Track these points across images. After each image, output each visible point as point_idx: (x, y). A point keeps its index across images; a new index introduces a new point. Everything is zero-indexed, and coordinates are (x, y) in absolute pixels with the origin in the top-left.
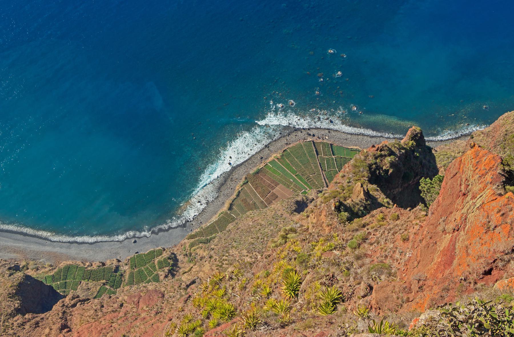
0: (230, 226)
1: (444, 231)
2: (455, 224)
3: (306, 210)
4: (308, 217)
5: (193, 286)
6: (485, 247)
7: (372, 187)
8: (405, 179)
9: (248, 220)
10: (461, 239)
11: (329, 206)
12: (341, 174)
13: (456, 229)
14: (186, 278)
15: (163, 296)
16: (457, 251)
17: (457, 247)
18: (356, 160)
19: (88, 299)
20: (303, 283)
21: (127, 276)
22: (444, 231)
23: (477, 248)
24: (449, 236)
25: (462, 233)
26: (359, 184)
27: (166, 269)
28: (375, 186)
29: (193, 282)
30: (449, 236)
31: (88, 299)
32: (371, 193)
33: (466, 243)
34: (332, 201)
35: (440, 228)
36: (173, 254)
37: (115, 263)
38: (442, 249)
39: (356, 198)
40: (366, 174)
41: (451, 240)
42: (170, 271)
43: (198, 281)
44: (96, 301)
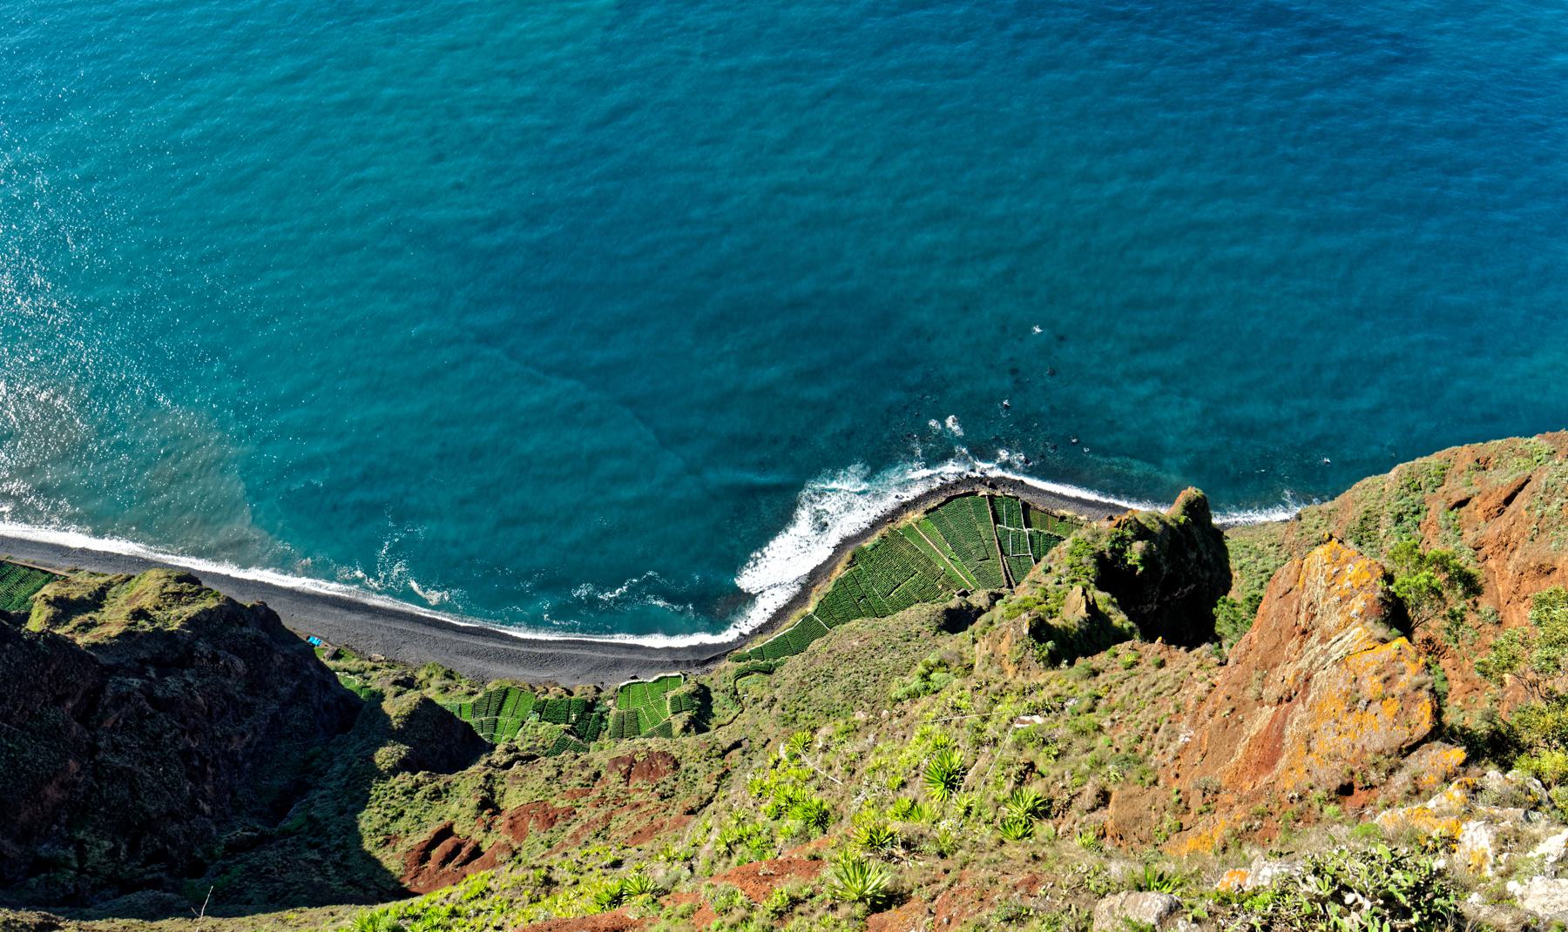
0: (816, 644)
1: (1259, 699)
2: (1284, 687)
3: (971, 628)
4: (975, 641)
5: (737, 752)
6: (1343, 738)
7: (1102, 598)
8: (1173, 590)
9: (854, 633)
10: (1296, 720)
11: (1017, 626)
12: (1042, 565)
13: (1285, 697)
14: (723, 737)
15: (677, 765)
16: (1287, 741)
17: (1287, 732)
18: (1077, 543)
19: (535, 757)
20: (970, 773)
21: (611, 719)
22: (1259, 699)
23: (1327, 741)
24: (1268, 711)
25: (1300, 707)
26: (1078, 589)
27: (685, 715)
28: (1107, 595)
29: (737, 745)
30: (1268, 711)
31: (535, 757)
32: (1100, 607)
33: (1308, 727)
34: (1024, 615)
35: (1251, 693)
36: (701, 686)
37: (591, 693)
38: (1253, 733)
39: (1072, 613)
40: (1091, 570)
41: (1274, 719)
42: (692, 721)
43: (745, 744)
44: (551, 761)
